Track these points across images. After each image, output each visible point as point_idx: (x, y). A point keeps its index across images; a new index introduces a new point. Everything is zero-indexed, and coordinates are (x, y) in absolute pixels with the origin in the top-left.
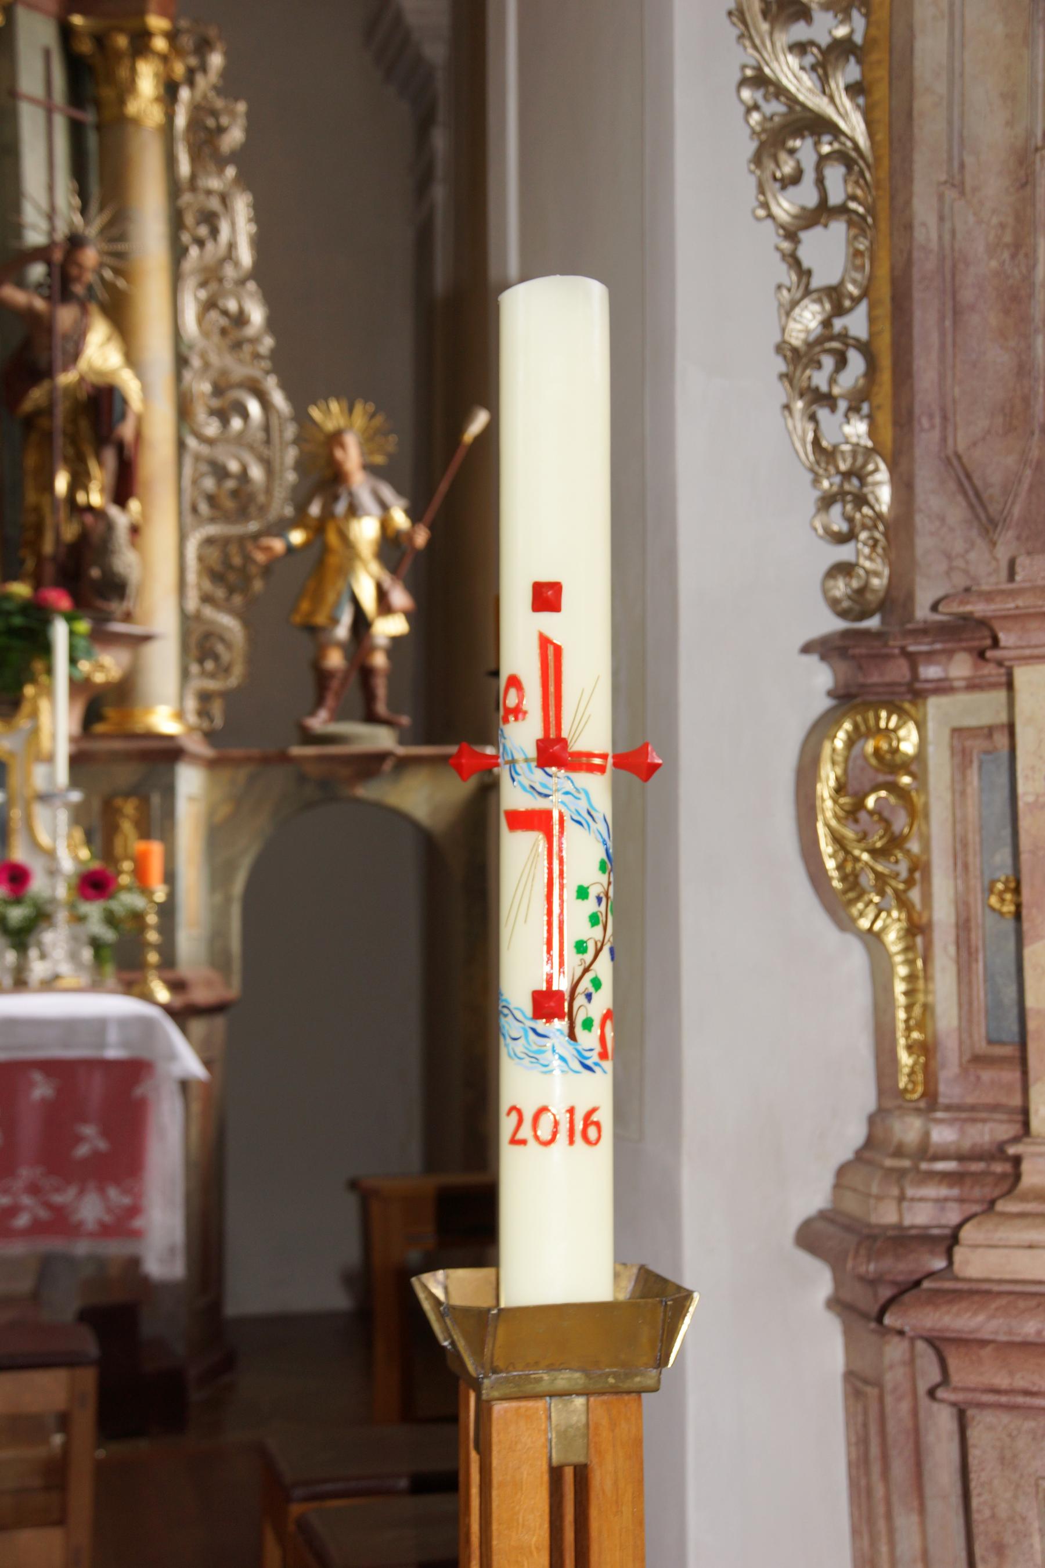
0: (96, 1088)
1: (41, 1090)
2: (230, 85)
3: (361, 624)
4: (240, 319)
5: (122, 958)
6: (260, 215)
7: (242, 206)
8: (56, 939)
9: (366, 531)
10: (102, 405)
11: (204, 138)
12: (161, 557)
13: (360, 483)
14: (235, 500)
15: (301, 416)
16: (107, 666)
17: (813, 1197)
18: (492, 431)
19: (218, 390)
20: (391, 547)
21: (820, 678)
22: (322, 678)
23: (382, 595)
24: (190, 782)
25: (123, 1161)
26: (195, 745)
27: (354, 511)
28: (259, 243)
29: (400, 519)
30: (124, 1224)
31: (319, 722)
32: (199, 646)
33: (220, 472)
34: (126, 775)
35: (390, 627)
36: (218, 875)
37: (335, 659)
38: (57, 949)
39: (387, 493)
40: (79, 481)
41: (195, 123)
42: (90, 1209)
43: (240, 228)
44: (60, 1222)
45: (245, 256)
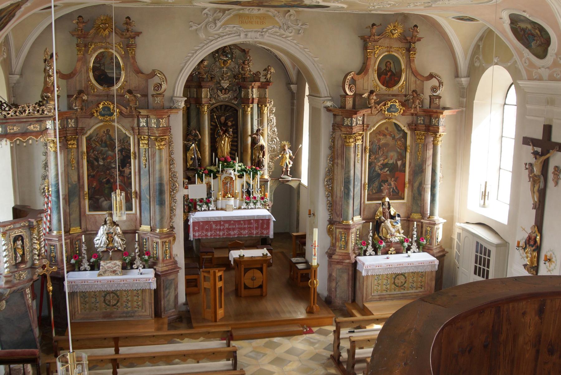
0: (265, 222)
1: (261, 222)
2: (273, 106)
3: (287, 166)
4: (274, 131)
5: (264, 205)
6: (277, 119)
7: (275, 118)
8: (259, 204)
9: (288, 156)
10: (262, 147)
11: (271, 111)
12: (266, 160)
13: (288, 150)
14: (274, 150)
15: (281, 141)
16: (262, 172)
17: (326, 250)
18: (302, 147)
19: (272, 138)
20: (290, 158)
21: (328, 223)
22: (283, 171)
23: (289, 163)
24: (269, 183)
25: (268, 228)
26: (269, 179)
27: (287, 154)
28: (276, 123)
29: (291, 154)
30: (268, 233)
31: (283, 176)
32: (269, 167)
33: (272, 148)
34: (263, 183)
35: (290, 166)
36: (271, 192)
37: (284, 170)
38: (259, 204)
39: (290, 151)
40: (259, 154)
41: (270, 110)
42: (265, 232)
43: (274, 121)
44: (262, 233)
45: (275, 124)
